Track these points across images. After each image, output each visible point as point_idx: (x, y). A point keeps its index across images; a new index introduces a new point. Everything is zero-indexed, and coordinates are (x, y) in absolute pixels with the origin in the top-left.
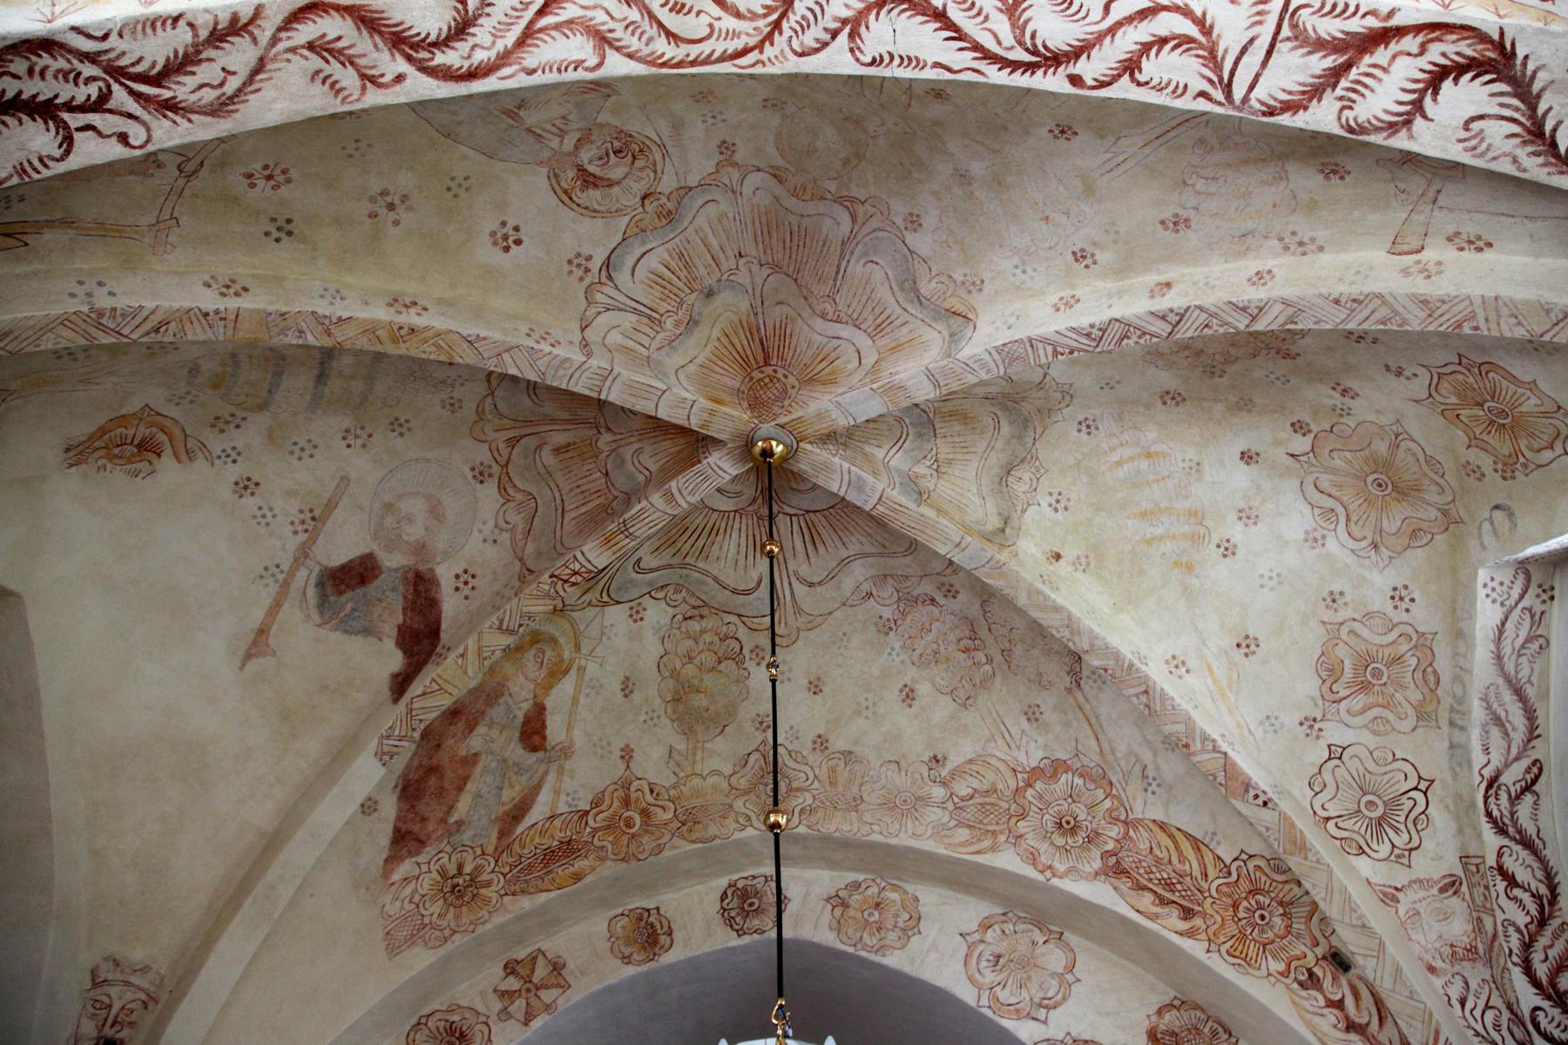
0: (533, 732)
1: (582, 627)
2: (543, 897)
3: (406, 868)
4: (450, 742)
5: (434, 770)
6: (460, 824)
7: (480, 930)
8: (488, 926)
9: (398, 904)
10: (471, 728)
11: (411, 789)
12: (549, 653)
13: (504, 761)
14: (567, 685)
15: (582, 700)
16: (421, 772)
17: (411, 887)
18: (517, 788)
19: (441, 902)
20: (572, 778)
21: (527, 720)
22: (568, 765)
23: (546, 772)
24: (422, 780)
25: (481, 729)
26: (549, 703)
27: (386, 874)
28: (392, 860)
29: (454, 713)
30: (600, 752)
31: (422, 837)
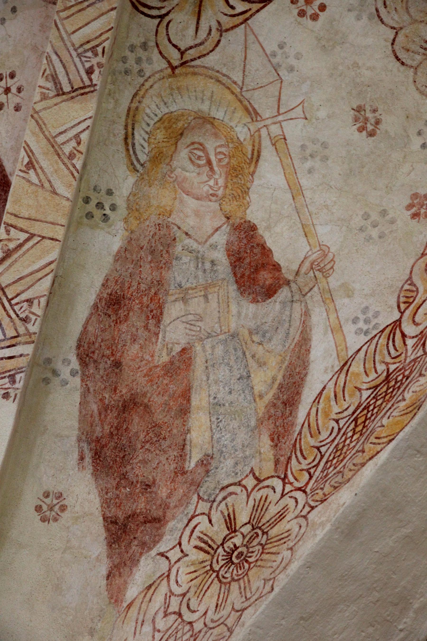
0: (254, 269)
1: (237, 76)
2: (369, 471)
3: (147, 567)
4: (134, 350)
5: (130, 405)
6: (205, 463)
7: (282, 580)
8: (294, 567)
9: (147, 628)
10: (156, 315)
11: (107, 453)
12: (211, 145)
13: (234, 336)
14: (269, 175)
15: (304, 182)
16: (111, 416)
17: (163, 589)
18: (273, 362)
19: (216, 585)
20: (349, 293)
21: (236, 259)
22: (334, 282)
23: (307, 314)
24: (118, 430)
25: (173, 310)
26: (255, 214)
27: (115, 595)
28: (119, 569)
29: (113, 303)
30: (375, 233)
31: (157, 513)
